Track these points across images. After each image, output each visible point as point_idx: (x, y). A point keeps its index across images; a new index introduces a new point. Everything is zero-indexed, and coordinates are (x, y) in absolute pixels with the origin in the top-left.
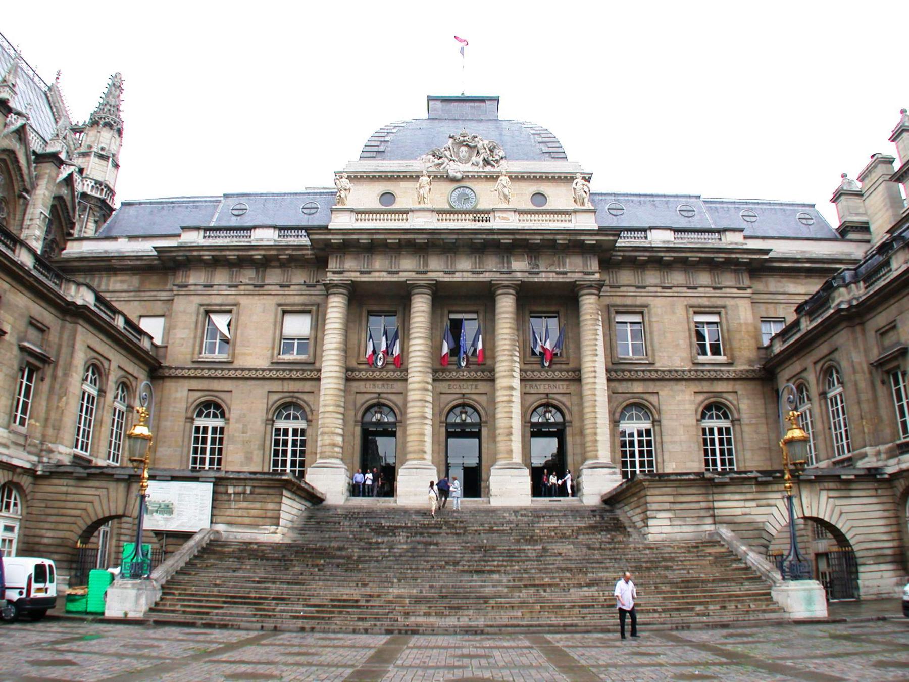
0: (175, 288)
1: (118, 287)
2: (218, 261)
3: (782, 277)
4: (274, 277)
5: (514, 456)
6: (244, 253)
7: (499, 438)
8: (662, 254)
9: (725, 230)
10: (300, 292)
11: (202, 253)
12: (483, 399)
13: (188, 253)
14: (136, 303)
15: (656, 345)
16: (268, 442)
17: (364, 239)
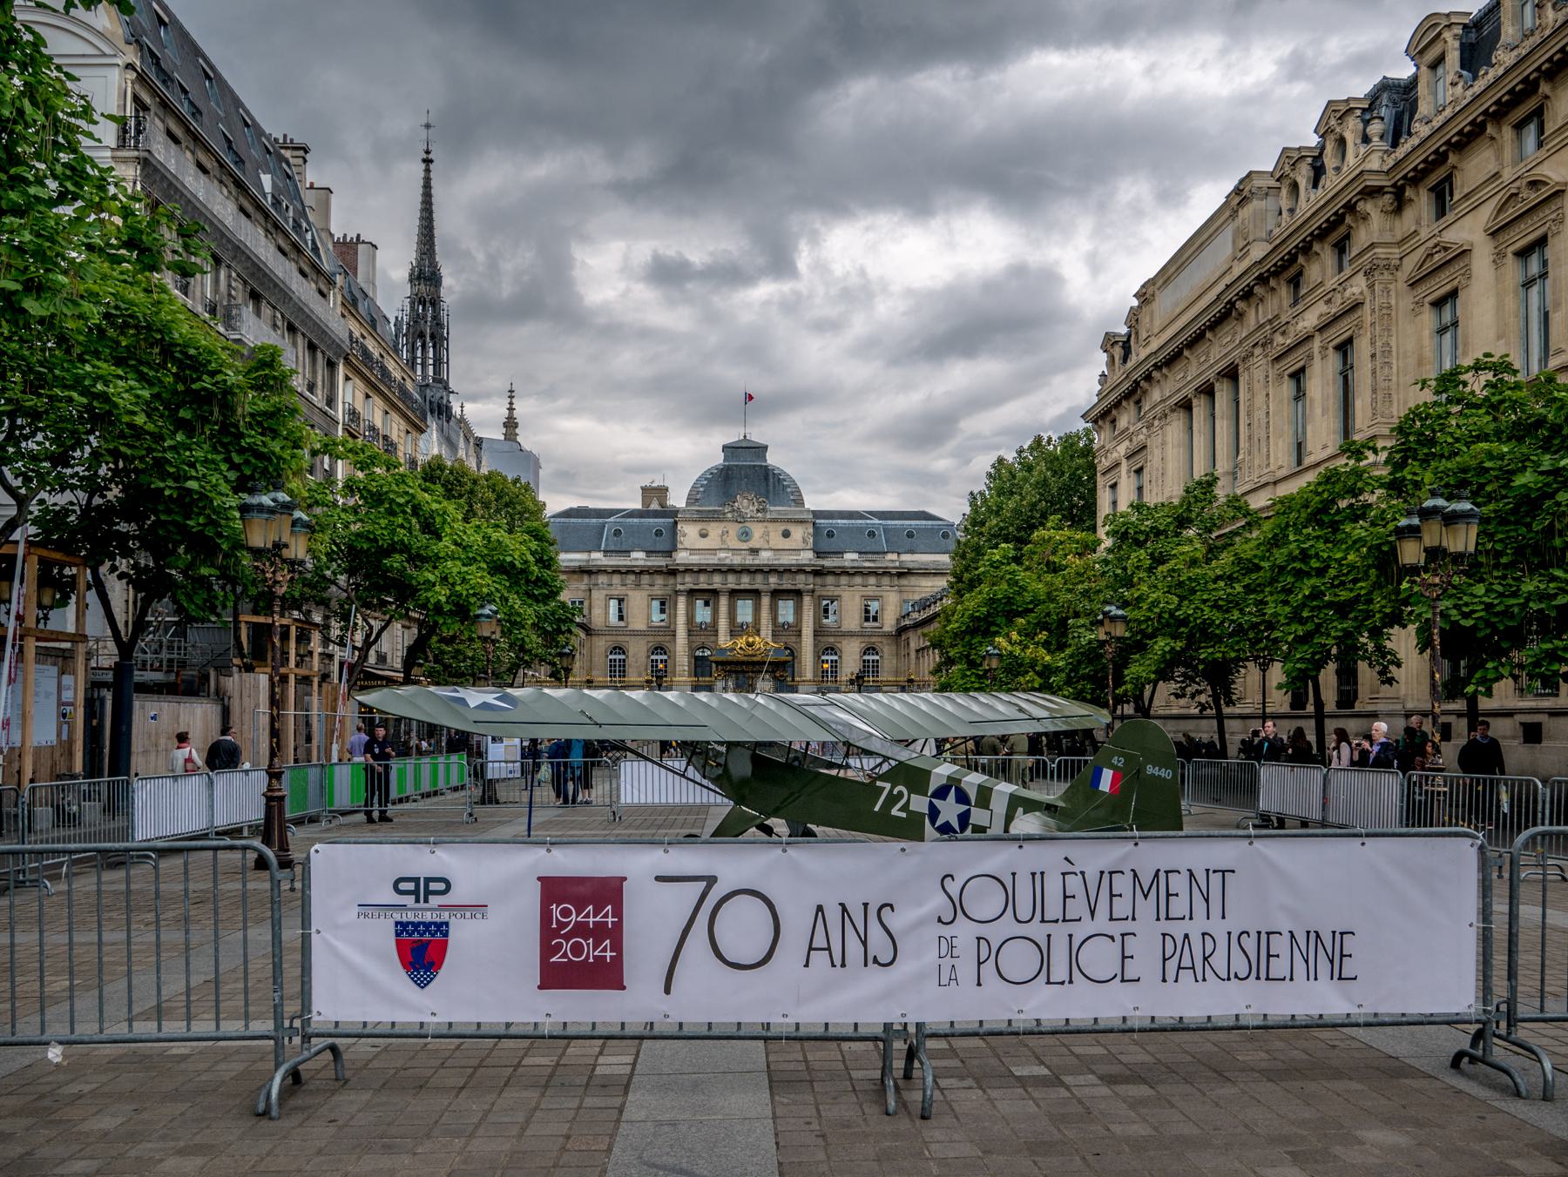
2: (616, 571)
4: (645, 579)
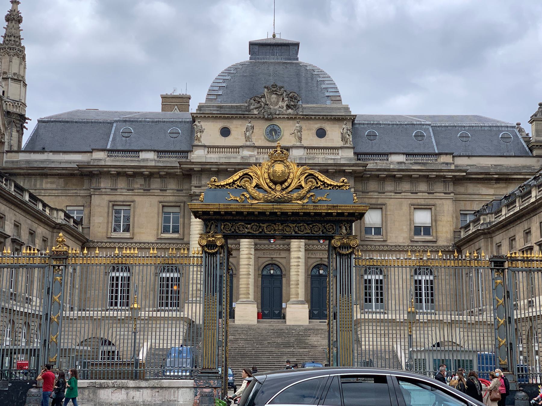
0: (92, 190)
1: (49, 186)
2: (121, 174)
3: (478, 183)
4: (156, 184)
5: (299, 297)
6: (138, 170)
7: (291, 287)
8: (395, 173)
9: (440, 154)
10: (173, 194)
11: (110, 169)
12: (283, 261)
13: (100, 169)
14: (63, 198)
15: (389, 229)
16: (156, 286)
17: (214, 168)
